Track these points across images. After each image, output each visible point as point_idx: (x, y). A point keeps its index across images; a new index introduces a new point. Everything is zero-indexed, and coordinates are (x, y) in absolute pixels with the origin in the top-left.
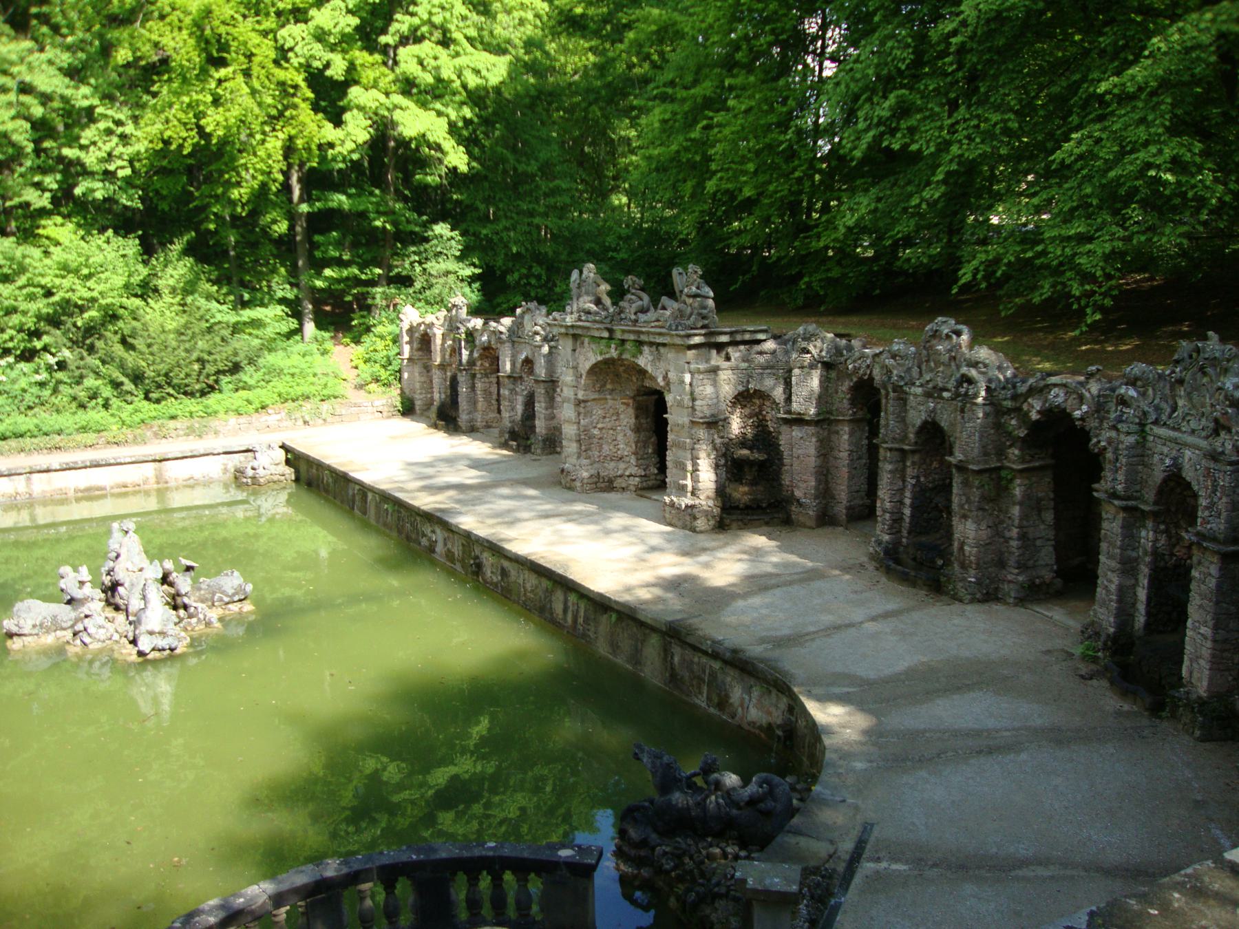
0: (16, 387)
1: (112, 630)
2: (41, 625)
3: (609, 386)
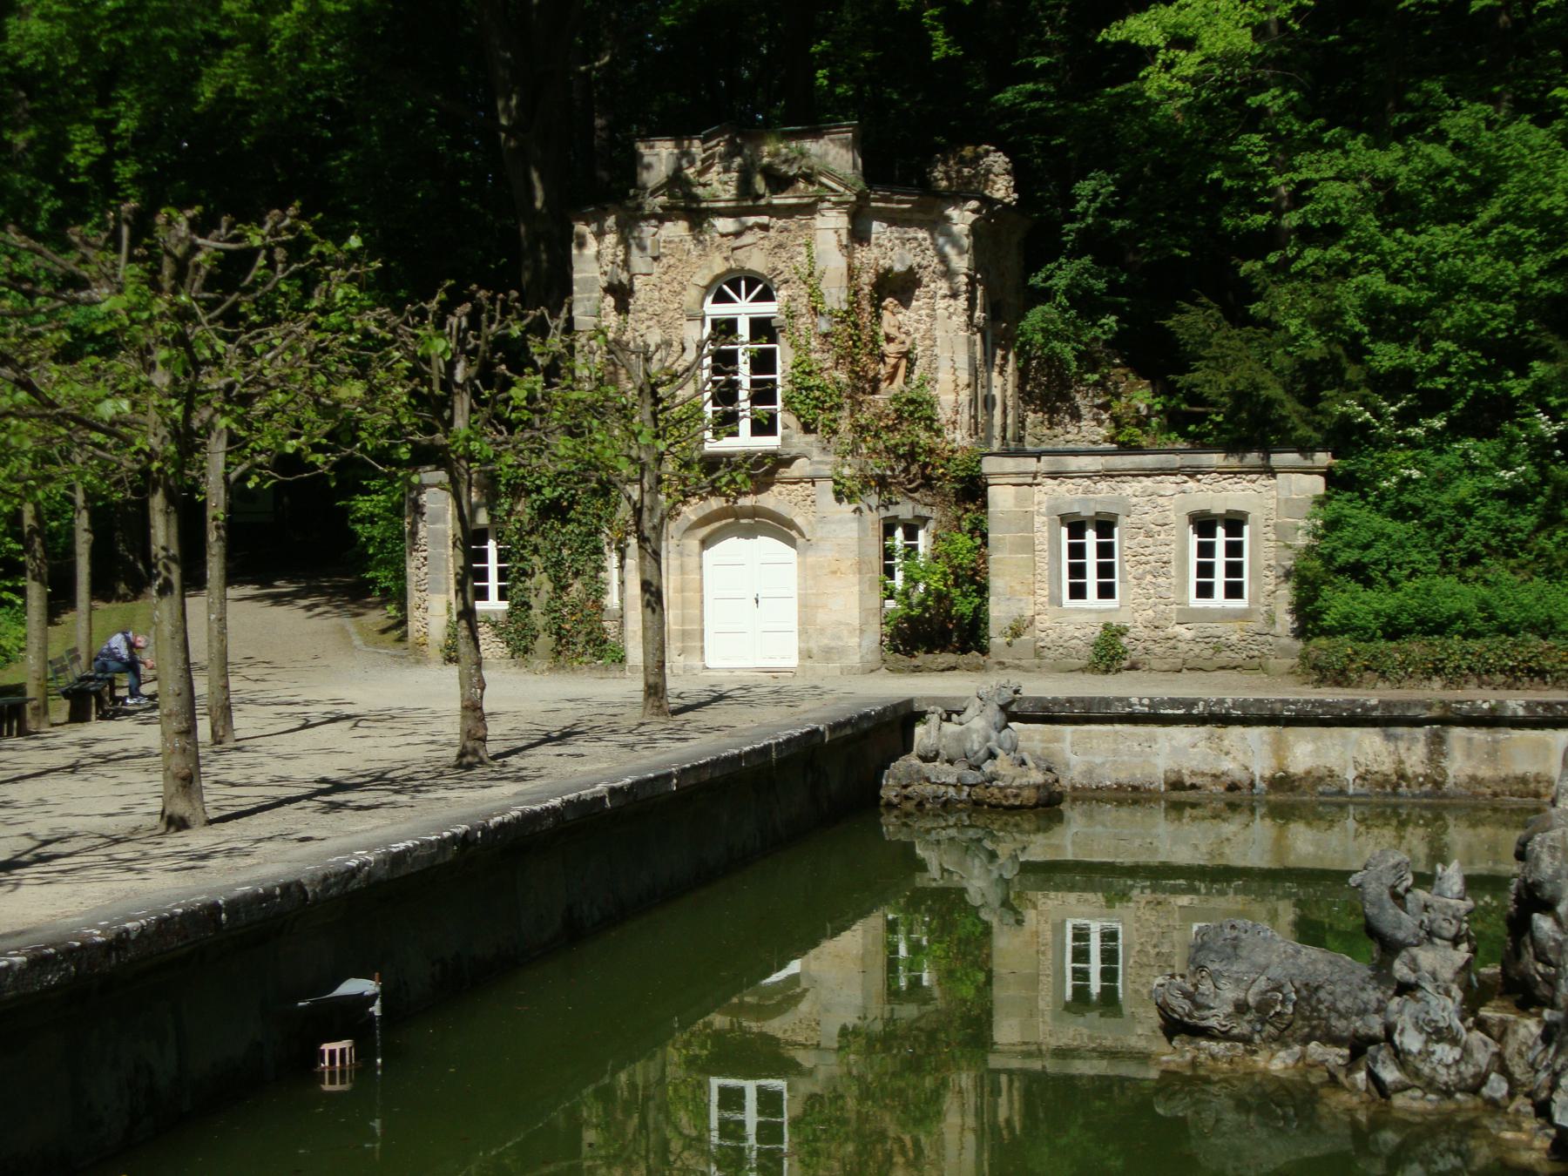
0: (1445, 498)
1: (1482, 1058)
2: (1263, 1006)
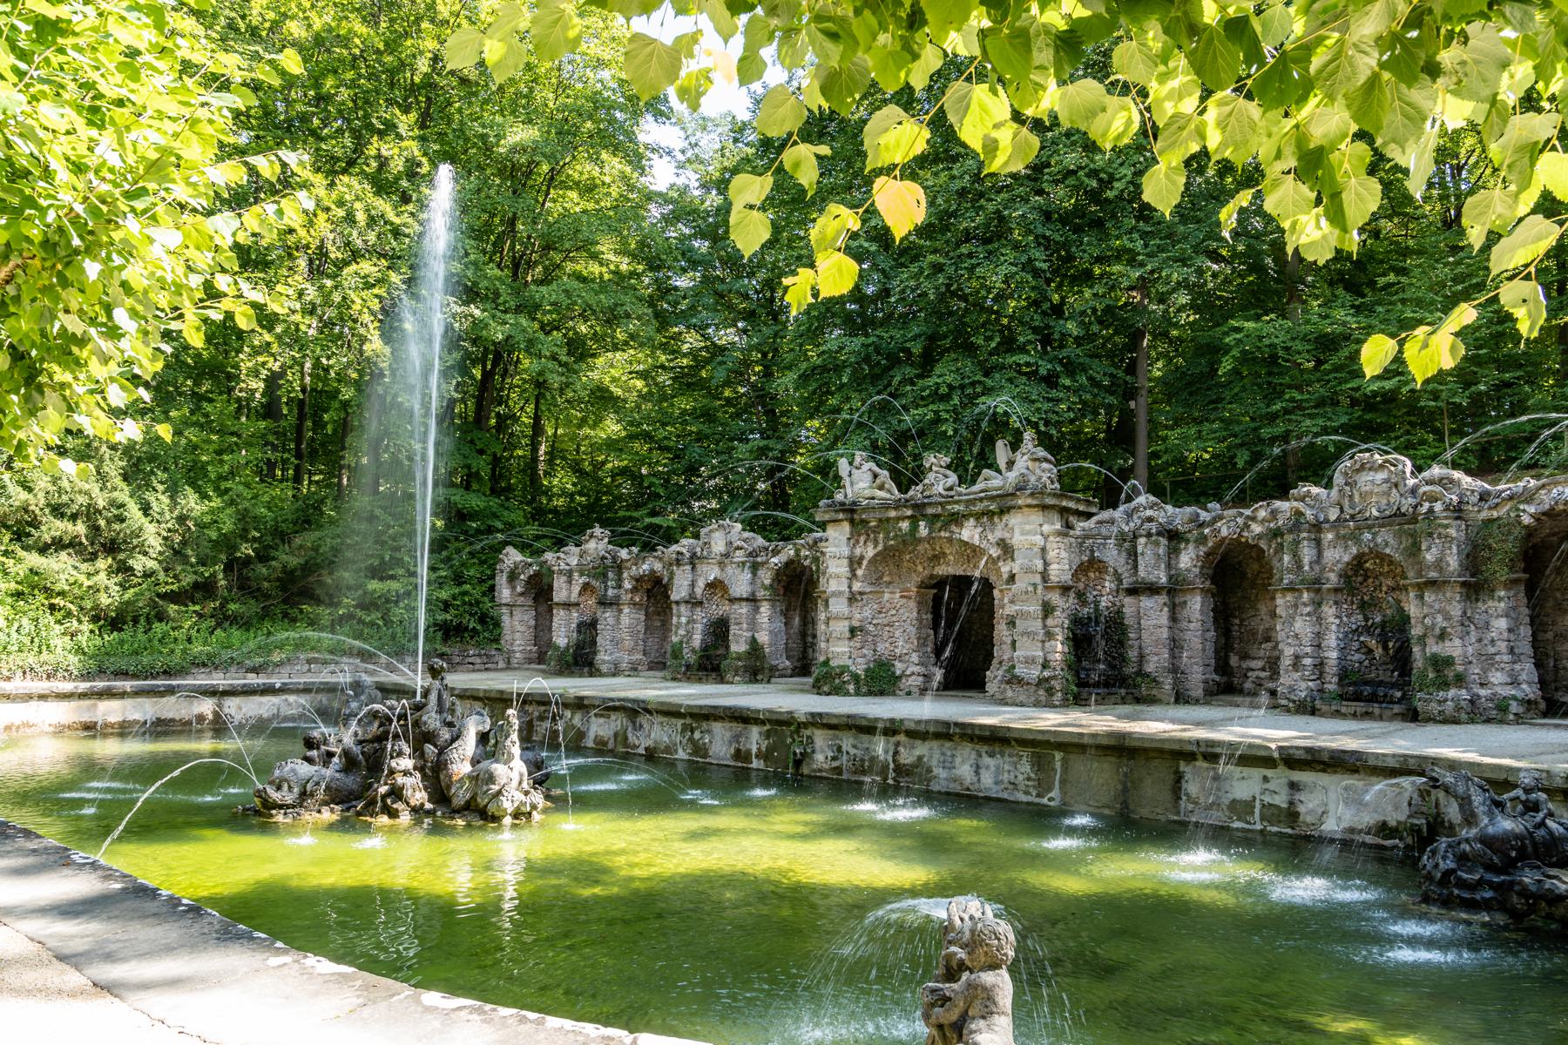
3: (886, 579)
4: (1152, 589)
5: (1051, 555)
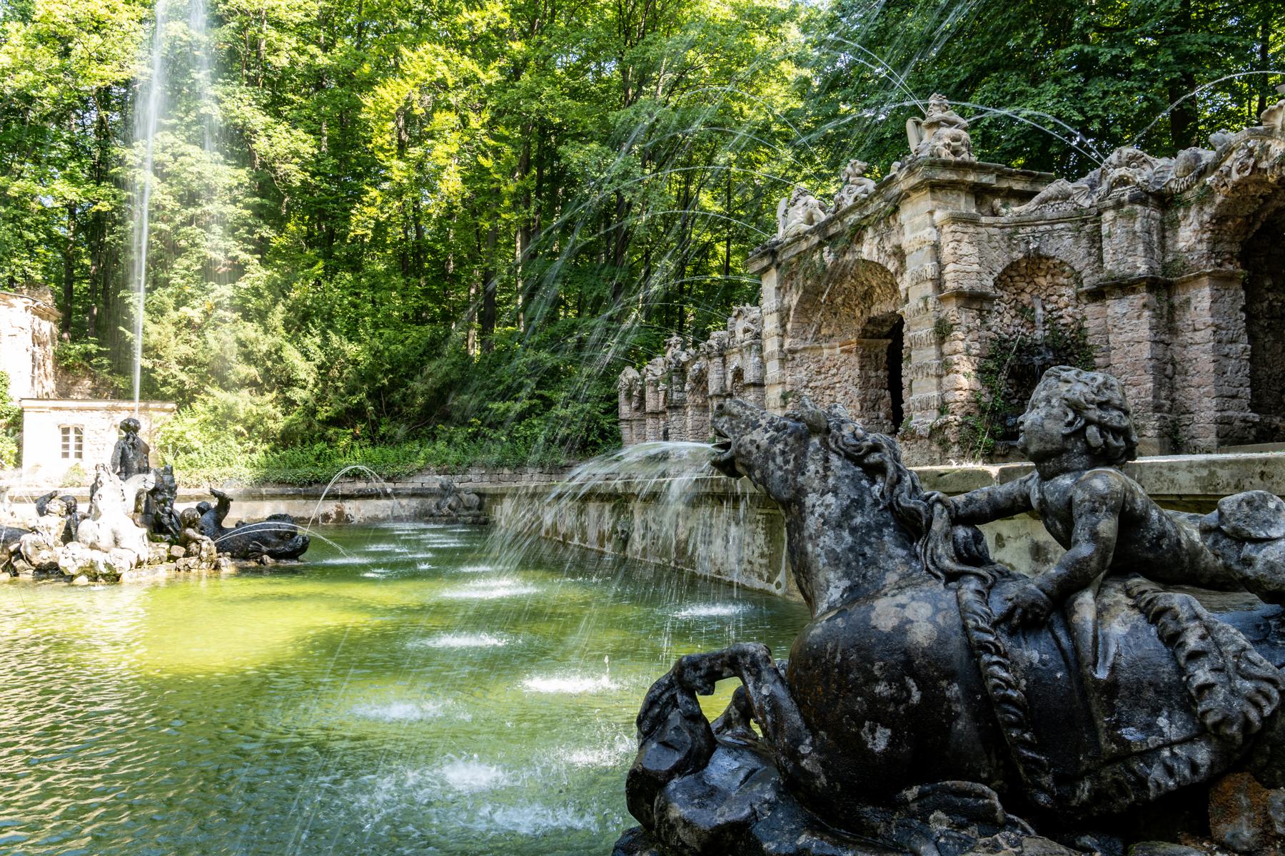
4: (1122, 286)
5: (947, 251)
